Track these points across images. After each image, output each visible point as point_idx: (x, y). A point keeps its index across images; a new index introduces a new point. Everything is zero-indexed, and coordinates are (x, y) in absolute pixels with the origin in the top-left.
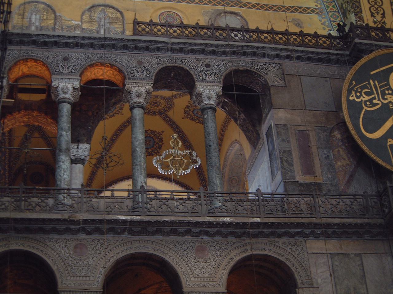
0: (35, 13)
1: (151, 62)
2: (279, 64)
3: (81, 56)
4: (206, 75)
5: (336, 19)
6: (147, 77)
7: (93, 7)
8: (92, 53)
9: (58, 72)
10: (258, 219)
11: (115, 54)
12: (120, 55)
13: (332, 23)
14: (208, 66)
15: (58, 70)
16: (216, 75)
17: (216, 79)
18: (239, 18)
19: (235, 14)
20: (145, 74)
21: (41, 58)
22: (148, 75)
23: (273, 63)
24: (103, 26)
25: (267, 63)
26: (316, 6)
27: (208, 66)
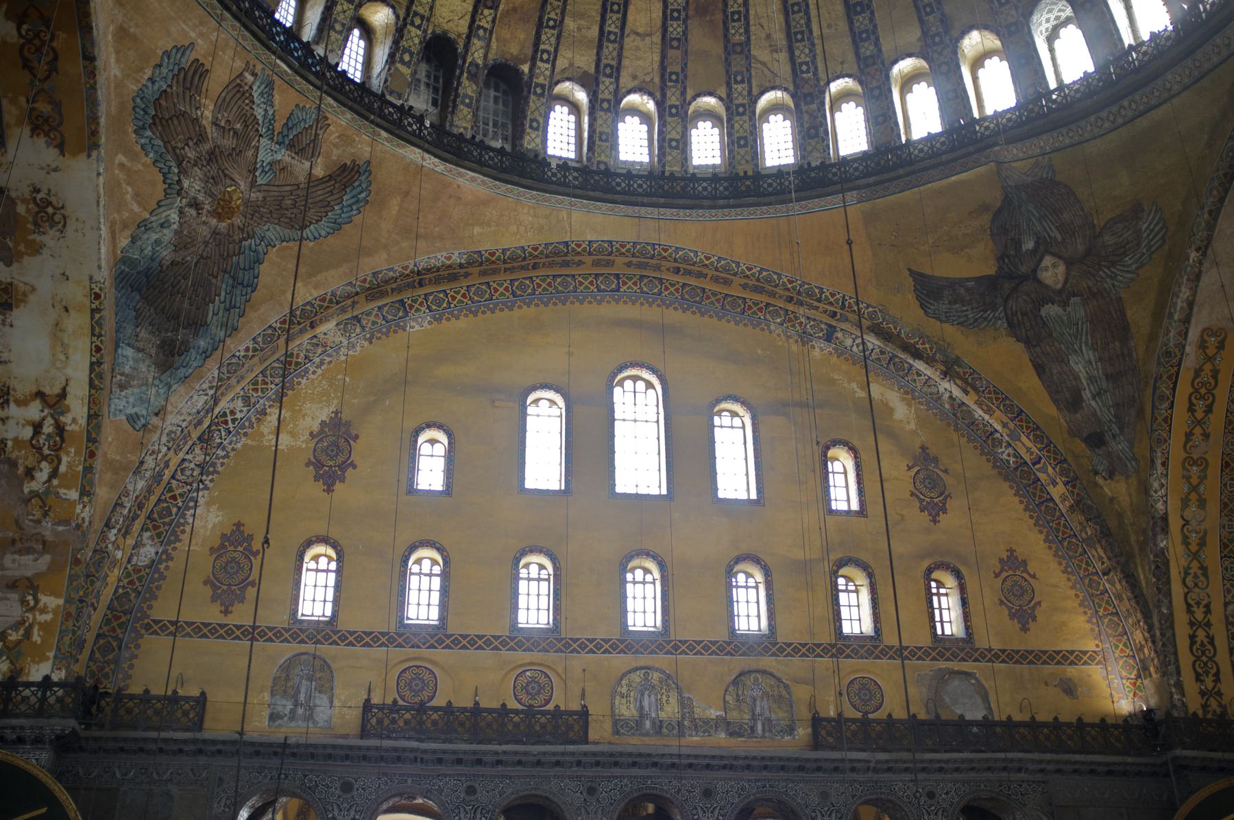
0: (647, 692)
2: (1044, 782)
3: (732, 787)
5: (1130, 674)
7: (740, 675)
8: (749, 781)
11: (785, 780)
12: (793, 782)
13: (1124, 681)
16: (945, 814)
18: (973, 681)
19: (967, 674)
21: (667, 792)
25: (1023, 781)
26: (1097, 646)
27: (931, 795)
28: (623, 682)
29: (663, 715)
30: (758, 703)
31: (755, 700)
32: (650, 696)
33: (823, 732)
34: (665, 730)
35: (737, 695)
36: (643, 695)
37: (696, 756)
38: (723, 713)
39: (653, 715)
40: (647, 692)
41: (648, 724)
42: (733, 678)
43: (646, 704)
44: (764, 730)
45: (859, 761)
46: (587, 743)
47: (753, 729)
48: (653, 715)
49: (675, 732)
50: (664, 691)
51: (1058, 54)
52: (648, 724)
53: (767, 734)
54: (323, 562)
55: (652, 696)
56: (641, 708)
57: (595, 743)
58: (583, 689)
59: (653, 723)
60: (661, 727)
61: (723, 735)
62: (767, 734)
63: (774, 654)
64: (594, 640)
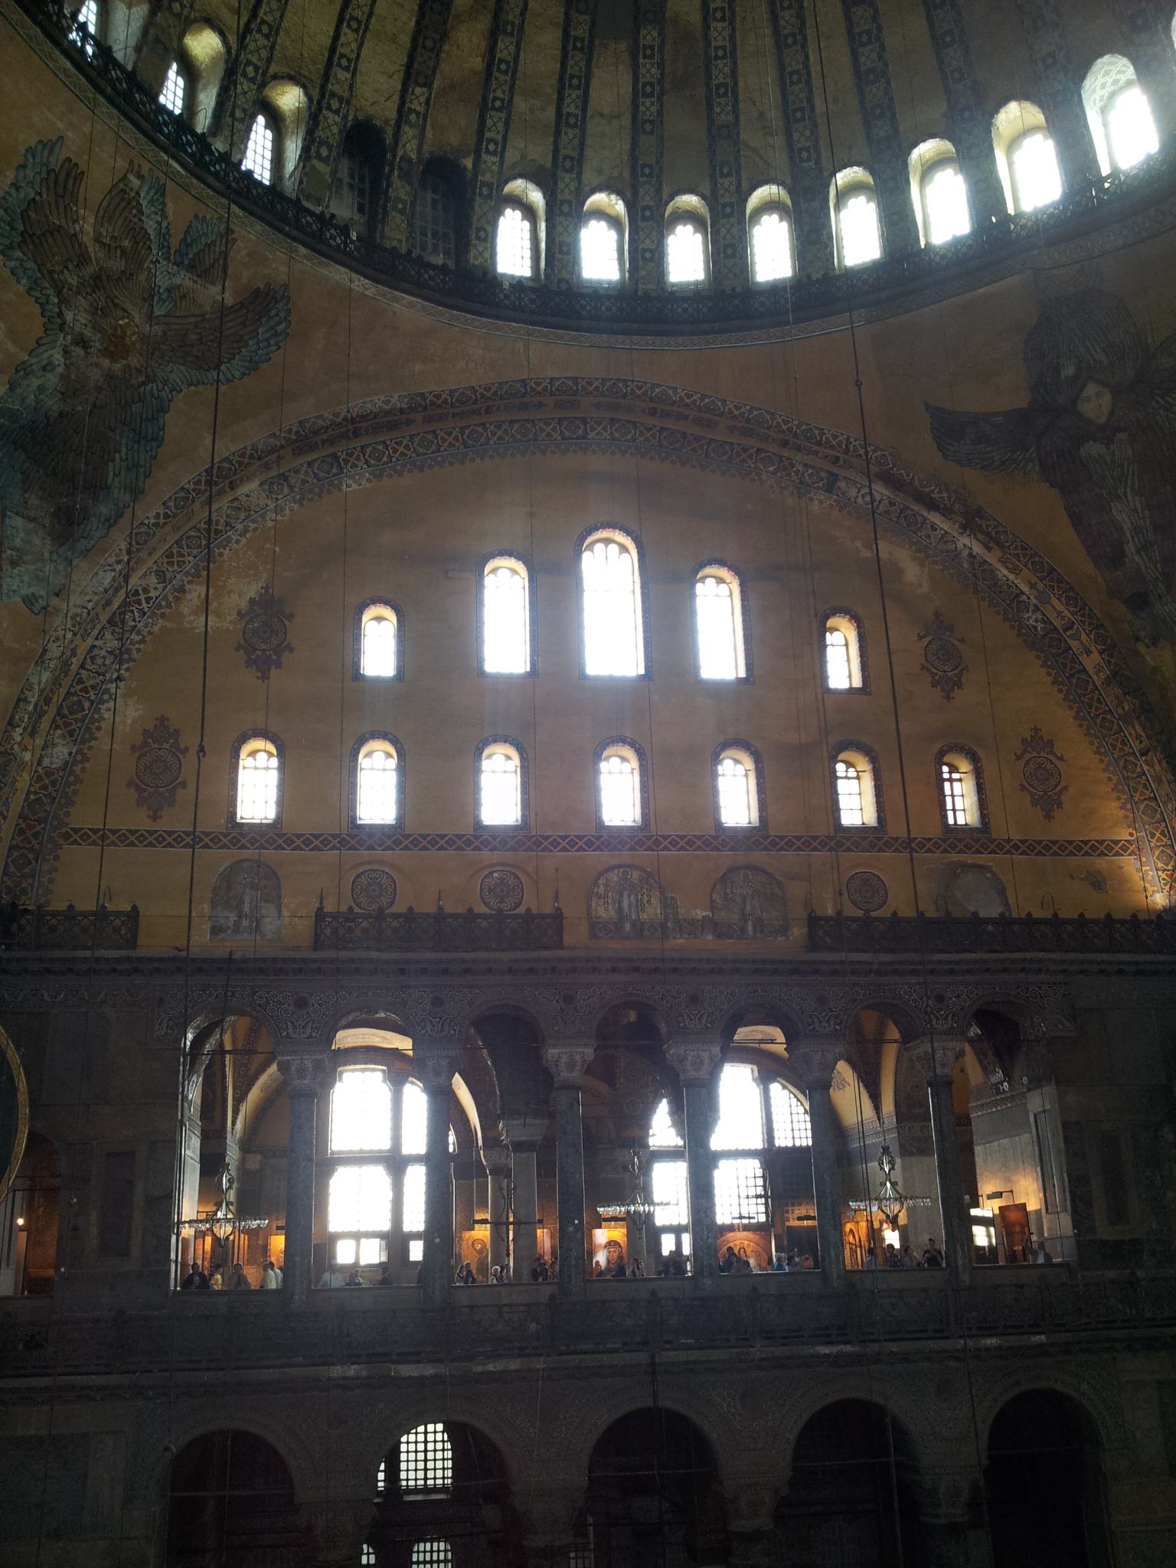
0: (626, 892)
1: (842, 997)
2: (1066, 984)
4: (938, 1019)
5: (1167, 865)
6: (836, 1030)
9: (683, 1027)
10: (1043, 1337)
13: (1160, 873)
14: (940, 999)
15: (682, 1025)
16: (956, 1018)
17: (955, 1025)
18: (989, 875)
19: (983, 868)
20: (832, 1026)
22: (838, 1027)
23: (1055, 984)
24: (749, 915)
25: (1042, 983)
26: (1131, 835)
27: (940, 999)
28: (600, 882)
29: (644, 916)
30: (748, 902)
31: (744, 898)
32: (629, 897)
33: (820, 933)
34: (646, 933)
35: (725, 893)
36: (622, 895)
37: (681, 960)
38: (709, 913)
39: (634, 916)
40: (626, 892)
41: (628, 926)
42: (720, 875)
43: (625, 904)
44: (755, 930)
45: (859, 962)
46: (562, 948)
47: (743, 930)
48: (634, 916)
49: (658, 934)
50: (644, 891)
51: (1017, 167)
52: (628, 926)
53: (759, 935)
54: (262, 757)
55: (632, 897)
56: (620, 909)
57: (573, 948)
58: (557, 892)
59: (633, 925)
60: (642, 930)
61: (710, 937)
62: (759, 935)
63: (766, 849)
64: (567, 837)
